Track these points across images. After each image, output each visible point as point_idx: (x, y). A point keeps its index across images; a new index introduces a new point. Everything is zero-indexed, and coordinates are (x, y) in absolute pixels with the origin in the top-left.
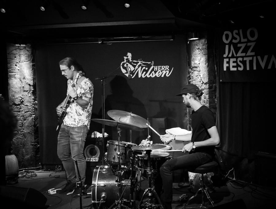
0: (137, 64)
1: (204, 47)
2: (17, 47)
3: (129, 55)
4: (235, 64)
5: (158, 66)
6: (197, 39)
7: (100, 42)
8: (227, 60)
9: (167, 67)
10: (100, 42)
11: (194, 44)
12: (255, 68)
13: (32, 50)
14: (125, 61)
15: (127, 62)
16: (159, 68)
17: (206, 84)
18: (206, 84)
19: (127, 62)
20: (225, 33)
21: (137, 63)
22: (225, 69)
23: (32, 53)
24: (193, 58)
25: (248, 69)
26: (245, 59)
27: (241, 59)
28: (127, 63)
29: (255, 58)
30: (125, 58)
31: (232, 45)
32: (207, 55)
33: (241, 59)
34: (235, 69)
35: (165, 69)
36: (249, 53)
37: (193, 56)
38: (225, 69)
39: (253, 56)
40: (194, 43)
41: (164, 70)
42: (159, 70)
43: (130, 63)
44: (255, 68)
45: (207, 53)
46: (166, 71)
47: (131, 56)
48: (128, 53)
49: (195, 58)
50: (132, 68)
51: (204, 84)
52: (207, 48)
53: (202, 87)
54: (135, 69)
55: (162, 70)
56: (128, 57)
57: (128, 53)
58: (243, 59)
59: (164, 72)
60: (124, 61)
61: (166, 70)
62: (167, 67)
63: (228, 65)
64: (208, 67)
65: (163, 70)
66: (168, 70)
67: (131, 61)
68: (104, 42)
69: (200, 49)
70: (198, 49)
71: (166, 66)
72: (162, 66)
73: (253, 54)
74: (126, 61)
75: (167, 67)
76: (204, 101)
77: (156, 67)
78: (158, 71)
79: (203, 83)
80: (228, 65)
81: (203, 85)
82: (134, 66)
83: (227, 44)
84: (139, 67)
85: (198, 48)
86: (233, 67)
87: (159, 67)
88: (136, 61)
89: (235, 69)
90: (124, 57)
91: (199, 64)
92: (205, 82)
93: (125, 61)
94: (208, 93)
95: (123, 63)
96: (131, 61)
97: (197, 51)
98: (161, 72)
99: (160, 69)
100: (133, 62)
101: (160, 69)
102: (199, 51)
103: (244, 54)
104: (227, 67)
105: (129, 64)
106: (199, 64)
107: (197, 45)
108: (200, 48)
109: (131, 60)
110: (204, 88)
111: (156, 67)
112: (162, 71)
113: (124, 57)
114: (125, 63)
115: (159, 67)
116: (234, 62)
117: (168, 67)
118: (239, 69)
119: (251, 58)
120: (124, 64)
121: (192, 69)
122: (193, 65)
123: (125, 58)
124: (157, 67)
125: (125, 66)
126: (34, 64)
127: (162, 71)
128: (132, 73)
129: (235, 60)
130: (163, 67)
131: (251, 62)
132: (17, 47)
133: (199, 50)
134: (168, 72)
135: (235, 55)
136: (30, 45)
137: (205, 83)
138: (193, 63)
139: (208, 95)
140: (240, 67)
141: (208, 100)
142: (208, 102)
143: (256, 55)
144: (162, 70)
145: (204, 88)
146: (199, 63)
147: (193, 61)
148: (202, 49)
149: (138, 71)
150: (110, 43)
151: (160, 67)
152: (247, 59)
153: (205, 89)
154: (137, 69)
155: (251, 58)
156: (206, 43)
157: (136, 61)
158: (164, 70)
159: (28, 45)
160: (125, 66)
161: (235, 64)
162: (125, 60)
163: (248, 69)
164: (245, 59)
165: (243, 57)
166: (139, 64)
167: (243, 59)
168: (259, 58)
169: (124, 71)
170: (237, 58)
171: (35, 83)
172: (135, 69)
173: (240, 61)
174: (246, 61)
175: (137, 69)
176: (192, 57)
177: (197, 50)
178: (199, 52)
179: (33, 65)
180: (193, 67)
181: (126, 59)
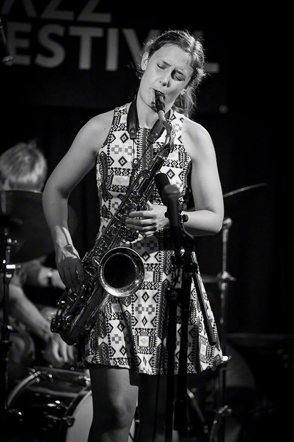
4: (25, 44)
12: (112, 64)
25: (85, 63)
26: (74, 31)
27: (59, 31)
29: (113, 34)
33: (59, 31)
34: (25, 60)
36: (87, 15)
39: (105, 27)
44: (112, 64)
58: (67, 32)
73: (106, 18)
86: (20, 51)
89: (25, 60)
103: (69, 16)
116: (19, 35)
118: (43, 61)
119: (98, 32)
129: (26, 28)
131: (99, 48)
135: (31, 12)
140: (49, 54)
143: (119, 23)
152: (87, 36)
155: (98, 32)
161: (25, 44)
163: (85, 63)
164: (74, 31)
165: (66, 24)
167: (67, 32)
168: (131, 35)
170: (38, 23)
173: (53, 37)
174: (77, 40)
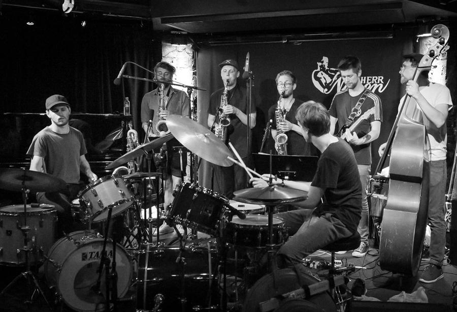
0: (336, 74)
2: (175, 49)
3: (326, 60)
5: (366, 76)
7: (284, 42)
9: (381, 79)
10: (284, 42)
11: (425, 43)
13: (193, 53)
14: (319, 70)
15: (321, 70)
16: (368, 80)
19: (321, 70)
21: (335, 72)
23: (193, 57)
28: (322, 72)
30: (319, 64)
32: (446, 61)
35: (377, 81)
40: (425, 42)
41: (376, 82)
42: (368, 83)
43: (326, 72)
46: (378, 84)
50: (329, 80)
54: (332, 81)
55: (373, 82)
56: (322, 62)
59: (376, 86)
60: (317, 69)
61: (378, 82)
62: (381, 78)
64: (446, 79)
65: (374, 83)
66: (382, 82)
67: (327, 68)
68: (290, 41)
71: (379, 77)
72: (373, 77)
75: (381, 78)
77: (363, 79)
78: (366, 83)
82: (332, 77)
84: (338, 78)
87: (368, 78)
88: (334, 69)
93: (319, 70)
95: (316, 72)
98: (370, 85)
99: (369, 81)
100: (329, 70)
101: (369, 81)
105: (323, 73)
109: (328, 67)
111: (363, 79)
112: (372, 84)
114: (319, 72)
115: (368, 78)
117: (383, 78)
123: (319, 64)
124: (365, 78)
125: (319, 75)
126: (196, 72)
127: (372, 84)
128: (327, 86)
130: (375, 78)
132: (175, 49)
134: (381, 85)
136: (191, 46)
144: (373, 82)
149: (337, 84)
150: (297, 43)
151: (370, 78)
154: (335, 81)
157: (334, 69)
158: (376, 82)
159: (189, 45)
160: (319, 75)
162: (318, 66)
166: (338, 73)
169: (316, 84)
171: (196, 98)
172: (332, 81)
175: (335, 81)
179: (194, 74)
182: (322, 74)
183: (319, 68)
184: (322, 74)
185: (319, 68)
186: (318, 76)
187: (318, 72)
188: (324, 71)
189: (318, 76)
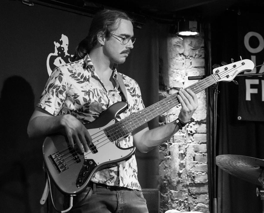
1: (197, 53)
3: (65, 39)
6: (195, 33)
8: (256, 82)
11: (171, 44)
14: (56, 54)
15: (59, 55)
17: (200, 123)
18: (200, 123)
19: (59, 55)
20: (250, 34)
22: (248, 98)
24: (172, 70)
28: (60, 58)
31: (240, 56)
32: (203, 69)
37: (172, 66)
38: (248, 98)
45: (203, 65)
47: (68, 44)
48: (63, 35)
49: (175, 71)
51: (194, 123)
52: (203, 56)
53: (188, 129)
56: (61, 43)
57: (63, 35)
60: (54, 52)
63: (255, 91)
67: (66, 54)
69: (185, 56)
70: (180, 54)
74: (58, 53)
76: (194, 158)
79: (192, 120)
80: (255, 91)
81: (191, 125)
83: (254, 54)
85: (181, 52)
90: (55, 42)
91: (183, 83)
92: (199, 120)
93: (56, 54)
94: (205, 141)
95: (52, 56)
96: (66, 54)
97: (180, 58)
100: (70, 57)
102: (183, 59)
104: (252, 95)
105: (62, 61)
106: (183, 83)
107: (179, 46)
108: (187, 54)
109: (68, 52)
110: (194, 132)
113: (55, 42)
120: (53, 59)
121: (168, 91)
122: (172, 84)
123: (57, 45)
133: (182, 56)
137: (195, 122)
138: (171, 79)
139: (205, 145)
141: (206, 154)
142: (206, 158)
145: (194, 132)
146: (183, 81)
147: (172, 77)
148: (191, 57)
153: (196, 133)
156: (203, 45)
176: (170, 66)
177: (178, 55)
178: (183, 61)
180: (171, 89)
181: (60, 49)
182: (61, 63)
183: (56, 51)
184: (61, 63)
185: (56, 51)
186: (54, 63)
187: (55, 57)
188: (62, 58)
189: (54, 63)
